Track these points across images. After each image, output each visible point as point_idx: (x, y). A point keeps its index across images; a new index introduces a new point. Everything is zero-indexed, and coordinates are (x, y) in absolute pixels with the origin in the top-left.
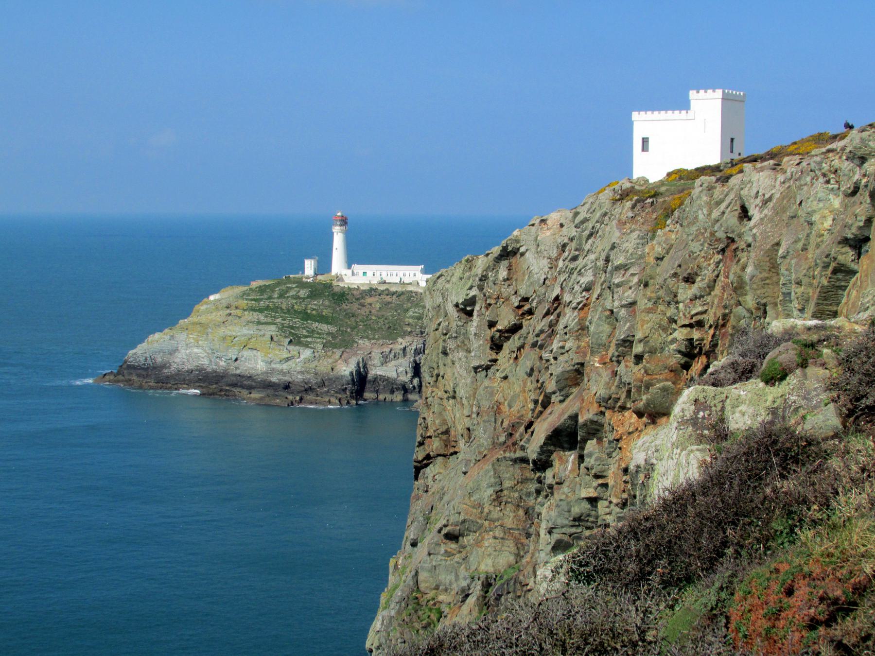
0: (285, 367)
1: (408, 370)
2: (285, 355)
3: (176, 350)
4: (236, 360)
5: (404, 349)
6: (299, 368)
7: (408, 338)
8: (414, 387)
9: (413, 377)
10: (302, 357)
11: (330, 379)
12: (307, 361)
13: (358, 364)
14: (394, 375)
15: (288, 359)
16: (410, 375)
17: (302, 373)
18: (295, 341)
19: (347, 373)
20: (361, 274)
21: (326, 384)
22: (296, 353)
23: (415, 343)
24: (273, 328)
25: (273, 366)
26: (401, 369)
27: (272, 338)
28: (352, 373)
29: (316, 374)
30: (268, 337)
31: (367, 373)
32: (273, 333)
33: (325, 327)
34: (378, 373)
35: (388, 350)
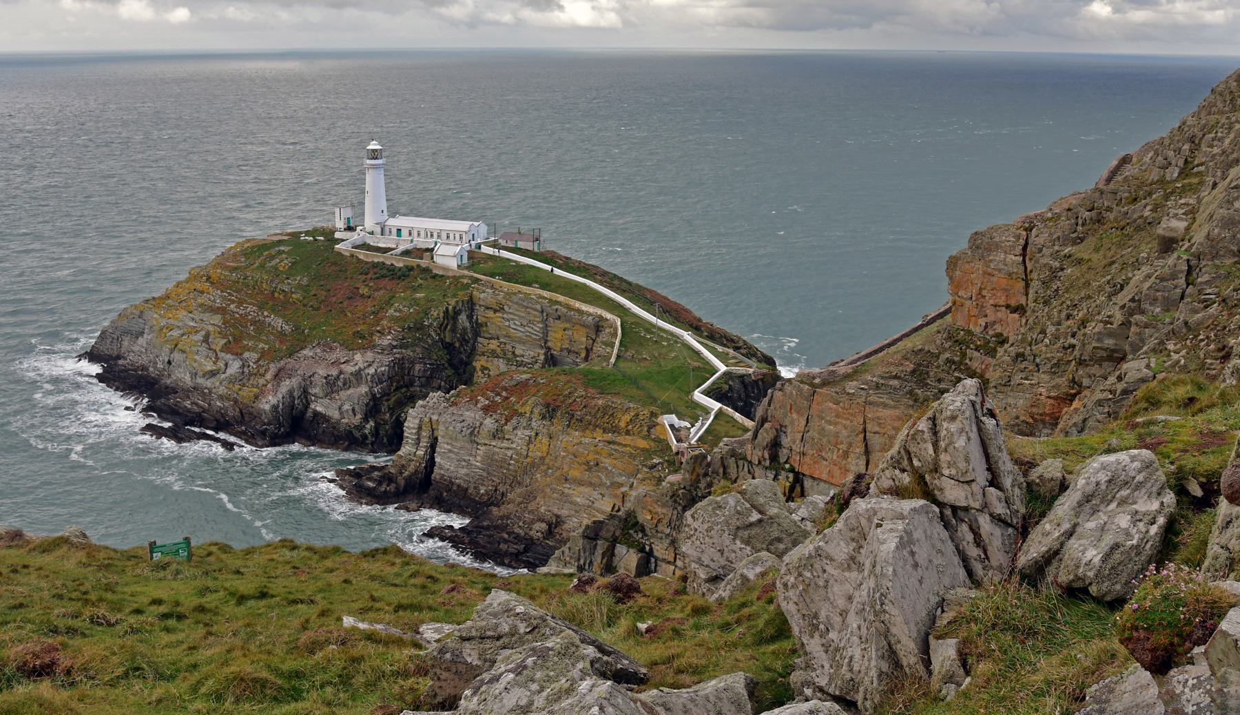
0: (208, 383)
1: (357, 408)
2: (209, 367)
3: (142, 333)
4: (169, 363)
5: (358, 375)
6: (222, 390)
7: (370, 355)
8: (365, 437)
9: (366, 419)
10: (229, 371)
11: (251, 414)
12: (232, 380)
13: (291, 393)
14: (335, 415)
15: (213, 374)
16: (359, 416)
17: (221, 398)
18: (234, 347)
19: (267, 407)
20: (394, 231)
21: (246, 419)
22: (221, 364)
23: (375, 365)
24: (217, 319)
25: (200, 381)
26: (346, 407)
27: (207, 336)
28: (275, 407)
29: (236, 401)
30: (199, 337)
31: (307, 406)
32: (211, 328)
33: (278, 323)
34: (319, 409)
35: (334, 372)
